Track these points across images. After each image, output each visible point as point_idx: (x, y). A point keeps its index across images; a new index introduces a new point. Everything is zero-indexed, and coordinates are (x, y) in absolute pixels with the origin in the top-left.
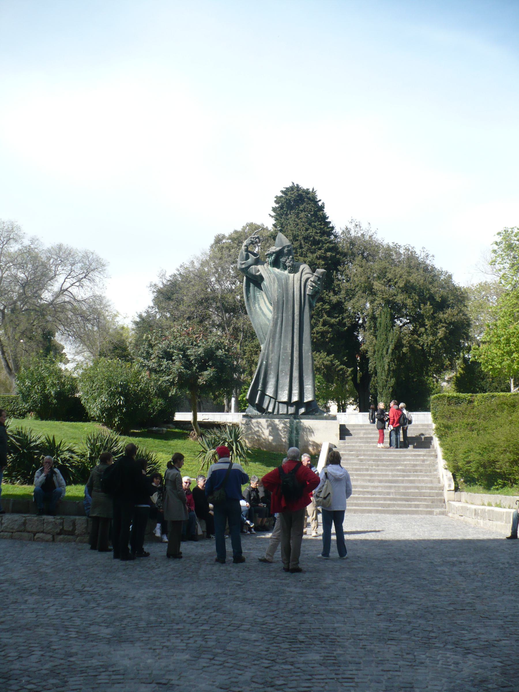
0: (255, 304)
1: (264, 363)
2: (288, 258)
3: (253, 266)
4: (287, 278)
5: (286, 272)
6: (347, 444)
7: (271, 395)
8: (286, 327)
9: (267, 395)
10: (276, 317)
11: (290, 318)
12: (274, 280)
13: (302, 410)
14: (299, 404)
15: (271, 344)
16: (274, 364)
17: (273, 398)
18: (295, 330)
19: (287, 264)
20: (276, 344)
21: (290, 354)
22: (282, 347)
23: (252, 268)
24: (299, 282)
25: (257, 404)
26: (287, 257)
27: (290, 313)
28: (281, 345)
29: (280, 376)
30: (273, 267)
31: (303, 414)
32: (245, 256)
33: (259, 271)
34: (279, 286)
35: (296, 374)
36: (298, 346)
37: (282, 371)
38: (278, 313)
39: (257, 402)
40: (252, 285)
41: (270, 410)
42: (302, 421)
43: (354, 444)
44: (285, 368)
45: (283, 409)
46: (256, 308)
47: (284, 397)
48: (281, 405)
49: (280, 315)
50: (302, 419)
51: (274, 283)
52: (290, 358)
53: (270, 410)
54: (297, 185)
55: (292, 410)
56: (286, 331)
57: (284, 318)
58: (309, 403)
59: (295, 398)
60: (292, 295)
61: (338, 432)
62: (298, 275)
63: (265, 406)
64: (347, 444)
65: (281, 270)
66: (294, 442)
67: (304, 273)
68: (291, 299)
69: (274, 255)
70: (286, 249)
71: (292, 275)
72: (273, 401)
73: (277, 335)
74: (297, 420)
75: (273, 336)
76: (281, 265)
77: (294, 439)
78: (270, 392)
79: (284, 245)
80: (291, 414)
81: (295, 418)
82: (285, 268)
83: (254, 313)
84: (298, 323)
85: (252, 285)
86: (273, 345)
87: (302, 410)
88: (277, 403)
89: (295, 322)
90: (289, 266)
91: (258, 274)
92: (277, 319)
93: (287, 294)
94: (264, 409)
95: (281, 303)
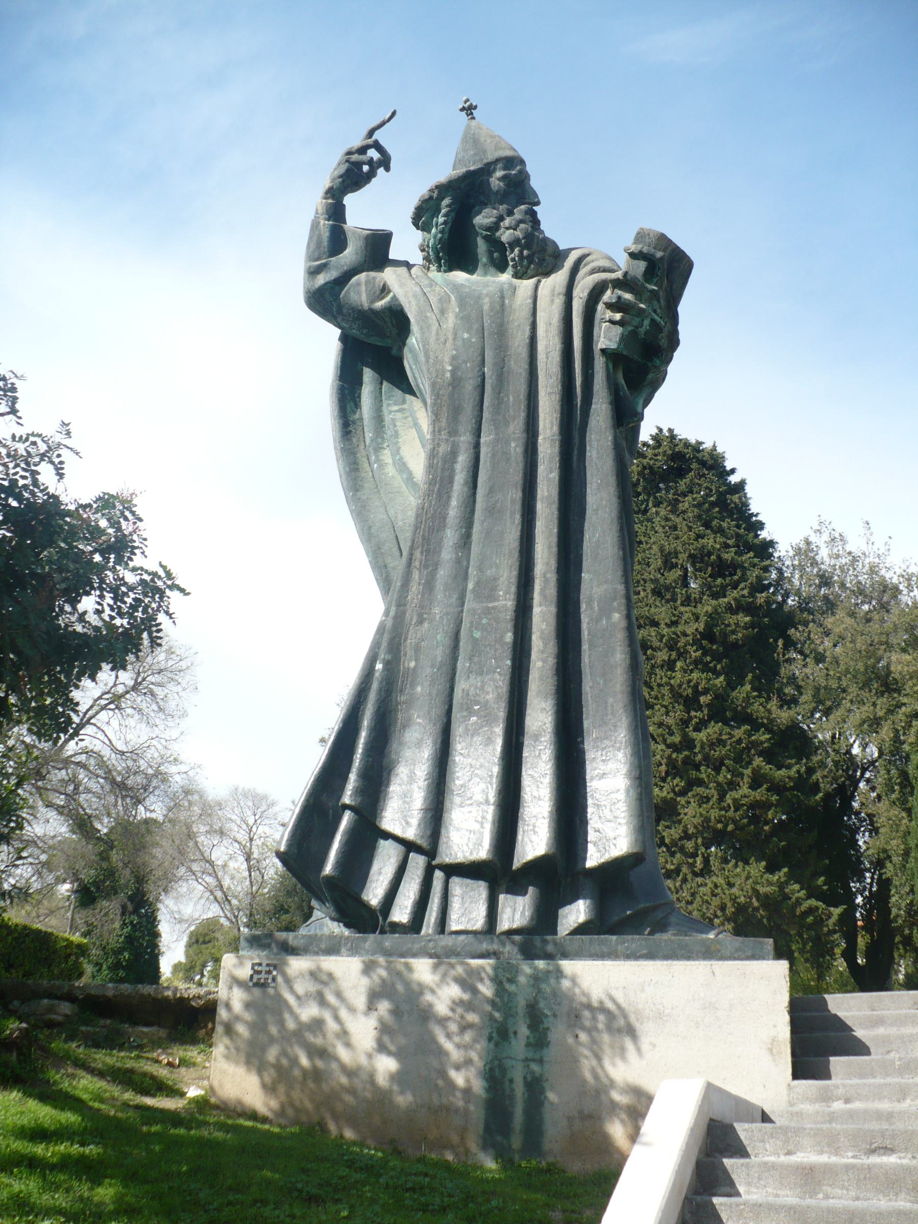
0: (378, 449)
1: (379, 666)
2: (510, 213)
3: (363, 276)
5: (505, 277)
6: (838, 1106)
7: (411, 833)
8: (491, 491)
9: (387, 836)
10: (443, 449)
11: (516, 449)
12: (444, 301)
13: (577, 913)
14: (559, 874)
15: (416, 575)
16: (427, 671)
17: (419, 849)
18: (540, 507)
19: (506, 236)
20: (443, 574)
21: (509, 615)
22: (470, 586)
23: (358, 284)
24: (559, 301)
25: (328, 879)
26: (503, 208)
27: (516, 427)
28: (466, 577)
29: (458, 730)
30: (450, 269)
31: (581, 930)
32: (326, 234)
33: (385, 290)
34: (464, 319)
35: (540, 717)
36: (553, 577)
38: (453, 432)
40: (368, 375)
41: (401, 914)
42: (567, 966)
43: (885, 1106)
44: (486, 687)
45: (468, 907)
46: (382, 466)
47: (469, 833)
48: (458, 886)
49: (465, 439)
50: (565, 956)
51: (443, 312)
52: (509, 637)
53: (401, 914)
54: (671, 431)
55: (516, 911)
56: (492, 511)
57: (484, 450)
58: (614, 870)
59: (535, 840)
60: (524, 352)
61: (785, 1032)
62: (559, 278)
63: (374, 895)
64: (838, 1106)
65: (485, 274)
66: (519, 1090)
67: (583, 271)
68: (519, 367)
69: (446, 201)
70: (499, 174)
71: (527, 285)
72: (417, 862)
73: (451, 536)
74: (541, 964)
75: (426, 540)
76: (482, 246)
77: (518, 1075)
78: (402, 814)
79: (491, 157)
80: (510, 933)
81: (529, 953)
82: (501, 267)
83: (368, 485)
84: (555, 475)
85: (368, 375)
86: (429, 585)
87: (577, 913)
88: (438, 875)
89: (542, 469)
90: (515, 243)
91: (379, 304)
92: (453, 455)
93: (502, 347)
94: (366, 906)
95: (469, 386)
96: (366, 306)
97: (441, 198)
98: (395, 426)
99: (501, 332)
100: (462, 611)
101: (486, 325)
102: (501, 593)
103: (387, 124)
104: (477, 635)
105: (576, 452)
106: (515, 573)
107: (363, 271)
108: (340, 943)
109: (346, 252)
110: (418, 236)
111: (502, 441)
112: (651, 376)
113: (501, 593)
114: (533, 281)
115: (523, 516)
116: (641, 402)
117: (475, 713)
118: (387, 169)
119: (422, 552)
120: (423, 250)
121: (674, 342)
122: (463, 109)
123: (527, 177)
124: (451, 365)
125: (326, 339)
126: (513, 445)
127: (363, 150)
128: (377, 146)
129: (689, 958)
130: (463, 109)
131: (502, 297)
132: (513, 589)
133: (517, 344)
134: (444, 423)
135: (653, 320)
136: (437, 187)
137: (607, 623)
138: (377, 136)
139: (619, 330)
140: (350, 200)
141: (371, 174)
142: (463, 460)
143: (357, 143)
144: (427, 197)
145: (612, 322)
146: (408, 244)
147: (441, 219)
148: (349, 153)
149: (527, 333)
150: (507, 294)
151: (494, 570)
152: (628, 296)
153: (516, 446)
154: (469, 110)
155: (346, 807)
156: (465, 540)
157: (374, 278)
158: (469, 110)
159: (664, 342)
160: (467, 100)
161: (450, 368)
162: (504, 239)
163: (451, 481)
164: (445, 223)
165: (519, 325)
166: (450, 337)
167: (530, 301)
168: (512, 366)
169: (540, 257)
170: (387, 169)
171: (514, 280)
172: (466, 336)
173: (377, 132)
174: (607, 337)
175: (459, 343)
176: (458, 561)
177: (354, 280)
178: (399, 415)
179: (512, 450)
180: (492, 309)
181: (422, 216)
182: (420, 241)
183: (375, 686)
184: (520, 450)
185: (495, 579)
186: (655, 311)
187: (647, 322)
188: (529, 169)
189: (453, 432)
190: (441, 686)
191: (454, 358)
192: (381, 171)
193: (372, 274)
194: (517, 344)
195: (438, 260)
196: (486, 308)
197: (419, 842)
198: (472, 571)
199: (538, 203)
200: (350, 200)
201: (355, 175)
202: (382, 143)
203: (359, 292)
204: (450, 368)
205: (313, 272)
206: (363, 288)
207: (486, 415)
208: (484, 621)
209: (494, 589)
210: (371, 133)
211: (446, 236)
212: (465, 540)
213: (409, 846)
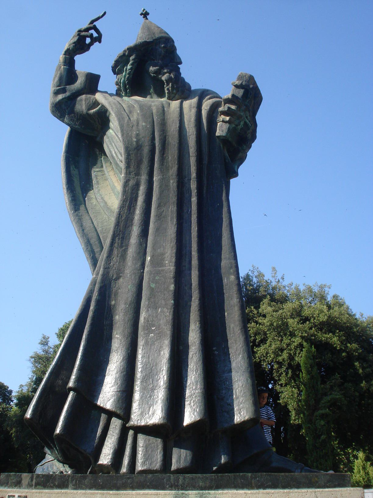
3: (84, 96)
4: (163, 112)
5: (164, 100)
8: (159, 206)
10: (132, 183)
15: (115, 252)
17: (118, 416)
22: (148, 258)
23: (81, 100)
28: (145, 254)
33: (96, 103)
37: (148, 329)
39: (58, 431)
41: (105, 458)
48: (142, 440)
49: (144, 178)
52: (172, 287)
53: (105, 458)
71: (175, 104)
73: (136, 230)
80: (179, 471)
86: (123, 257)
88: (131, 432)
92: (138, 185)
95: (146, 150)
96: (85, 111)
97: (130, 56)
98: (97, 178)
99: (163, 124)
100: (143, 272)
101: (155, 119)
102: (167, 262)
104: (153, 286)
105: (205, 188)
106: (175, 251)
107: (83, 94)
108: (68, 480)
109: (75, 84)
110: (114, 78)
111: (164, 180)
112: (240, 155)
113: (167, 262)
114: (179, 101)
115: (177, 220)
116: (236, 167)
117: (152, 332)
119: (119, 239)
121: (254, 137)
122: (141, 14)
124: (136, 138)
125: (61, 132)
126: (171, 182)
127: (87, 30)
129: (298, 487)
130: (141, 14)
131: (163, 107)
132: (174, 260)
133: (172, 130)
134: (132, 169)
135: (245, 122)
136: (128, 49)
137: (227, 281)
139: (227, 125)
142: (142, 189)
144: (122, 54)
145: (223, 121)
146: (109, 82)
147: (129, 67)
148: (80, 31)
149: (178, 125)
150: (166, 106)
151: (162, 249)
152: (233, 107)
153: (173, 183)
154: (145, 15)
155: (71, 389)
156: (144, 233)
157: (90, 98)
158: (145, 15)
159: (249, 136)
160: (144, 10)
161: (135, 140)
163: (136, 200)
164: (131, 69)
165: (173, 121)
166: (135, 123)
167: (178, 109)
168: (170, 141)
169: (182, 90)
170: (100, 42)
171: (168, 101)
172: (144, 124)
174: (221, 130)
175: (140, 128)
176: (140, 244)
177: (79, 98)
178: (99, 173)
179: (171, 184)
180: (158, 112)
181: (117, 67)
183: (90, 314)
184: (175, 184)
185: (163, 254)
186: (247, 117)
187: (242, 123)
189: (138, 174)
190: (130, 316)
191: (138, 135)
193: (89, 96)
194: (172, 130)
195: (125, 90)
196: (154, 111)
197: (118, 412)
198: (149, 250)
199: (181, 63)
201: (81, 45)
202: (98, 27)
203: (82, 104)
204: (135, 140)
205: (56, 93)
206: (84, 102)
207: (156, 165)
208: (157, 278)
209: (163, 259)
210: (92, 22)
211: (131, 76)
212: (144, 233)
213: (110, 414)
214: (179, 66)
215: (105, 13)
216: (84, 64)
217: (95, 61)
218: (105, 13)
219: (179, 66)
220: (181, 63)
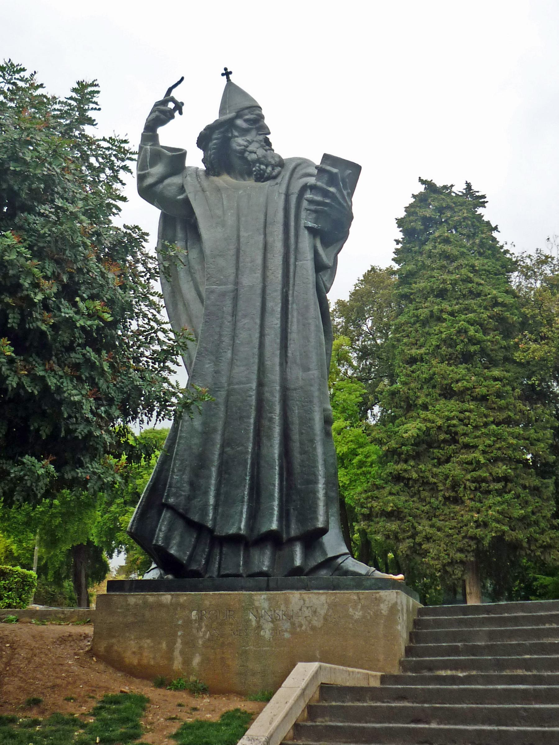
67: (296, 176)
103: (179, 86)
110: (200, 154)
118: (181, 113)
120: (204, 163)
121: (350, 218)
122: (223, 75)
123: (262, 117)
127: (164, 102)
128: (173, 100)
130: (223, 75)
138: (174, 94)
140: (161, 131)
141: (173, 117)
143: (161, 97)
146: (195, 159)
154: (227, 73)
162: (249, 158)
170: (181, 113)
173: (174, 90)
182: (202, 156)
188: (264, 112)
192: (177, 114)
199: (269, 133)
200: (161, 131)
210: (170, 90)
214: (268, 136)
215: (182, 79)
216: (169, 136)
217: (180, 134)
218: (182, 79)
219: (268, 136)
220: (269, 133)
